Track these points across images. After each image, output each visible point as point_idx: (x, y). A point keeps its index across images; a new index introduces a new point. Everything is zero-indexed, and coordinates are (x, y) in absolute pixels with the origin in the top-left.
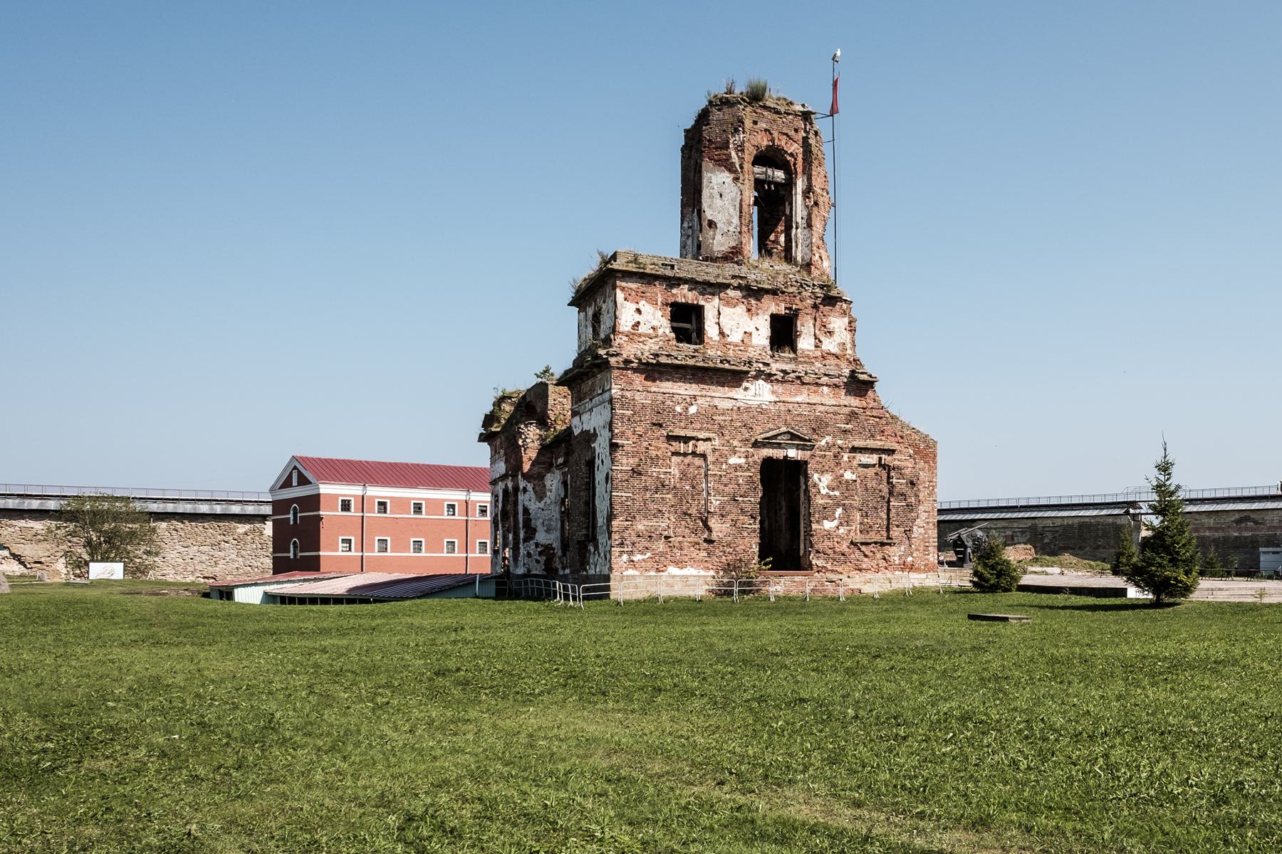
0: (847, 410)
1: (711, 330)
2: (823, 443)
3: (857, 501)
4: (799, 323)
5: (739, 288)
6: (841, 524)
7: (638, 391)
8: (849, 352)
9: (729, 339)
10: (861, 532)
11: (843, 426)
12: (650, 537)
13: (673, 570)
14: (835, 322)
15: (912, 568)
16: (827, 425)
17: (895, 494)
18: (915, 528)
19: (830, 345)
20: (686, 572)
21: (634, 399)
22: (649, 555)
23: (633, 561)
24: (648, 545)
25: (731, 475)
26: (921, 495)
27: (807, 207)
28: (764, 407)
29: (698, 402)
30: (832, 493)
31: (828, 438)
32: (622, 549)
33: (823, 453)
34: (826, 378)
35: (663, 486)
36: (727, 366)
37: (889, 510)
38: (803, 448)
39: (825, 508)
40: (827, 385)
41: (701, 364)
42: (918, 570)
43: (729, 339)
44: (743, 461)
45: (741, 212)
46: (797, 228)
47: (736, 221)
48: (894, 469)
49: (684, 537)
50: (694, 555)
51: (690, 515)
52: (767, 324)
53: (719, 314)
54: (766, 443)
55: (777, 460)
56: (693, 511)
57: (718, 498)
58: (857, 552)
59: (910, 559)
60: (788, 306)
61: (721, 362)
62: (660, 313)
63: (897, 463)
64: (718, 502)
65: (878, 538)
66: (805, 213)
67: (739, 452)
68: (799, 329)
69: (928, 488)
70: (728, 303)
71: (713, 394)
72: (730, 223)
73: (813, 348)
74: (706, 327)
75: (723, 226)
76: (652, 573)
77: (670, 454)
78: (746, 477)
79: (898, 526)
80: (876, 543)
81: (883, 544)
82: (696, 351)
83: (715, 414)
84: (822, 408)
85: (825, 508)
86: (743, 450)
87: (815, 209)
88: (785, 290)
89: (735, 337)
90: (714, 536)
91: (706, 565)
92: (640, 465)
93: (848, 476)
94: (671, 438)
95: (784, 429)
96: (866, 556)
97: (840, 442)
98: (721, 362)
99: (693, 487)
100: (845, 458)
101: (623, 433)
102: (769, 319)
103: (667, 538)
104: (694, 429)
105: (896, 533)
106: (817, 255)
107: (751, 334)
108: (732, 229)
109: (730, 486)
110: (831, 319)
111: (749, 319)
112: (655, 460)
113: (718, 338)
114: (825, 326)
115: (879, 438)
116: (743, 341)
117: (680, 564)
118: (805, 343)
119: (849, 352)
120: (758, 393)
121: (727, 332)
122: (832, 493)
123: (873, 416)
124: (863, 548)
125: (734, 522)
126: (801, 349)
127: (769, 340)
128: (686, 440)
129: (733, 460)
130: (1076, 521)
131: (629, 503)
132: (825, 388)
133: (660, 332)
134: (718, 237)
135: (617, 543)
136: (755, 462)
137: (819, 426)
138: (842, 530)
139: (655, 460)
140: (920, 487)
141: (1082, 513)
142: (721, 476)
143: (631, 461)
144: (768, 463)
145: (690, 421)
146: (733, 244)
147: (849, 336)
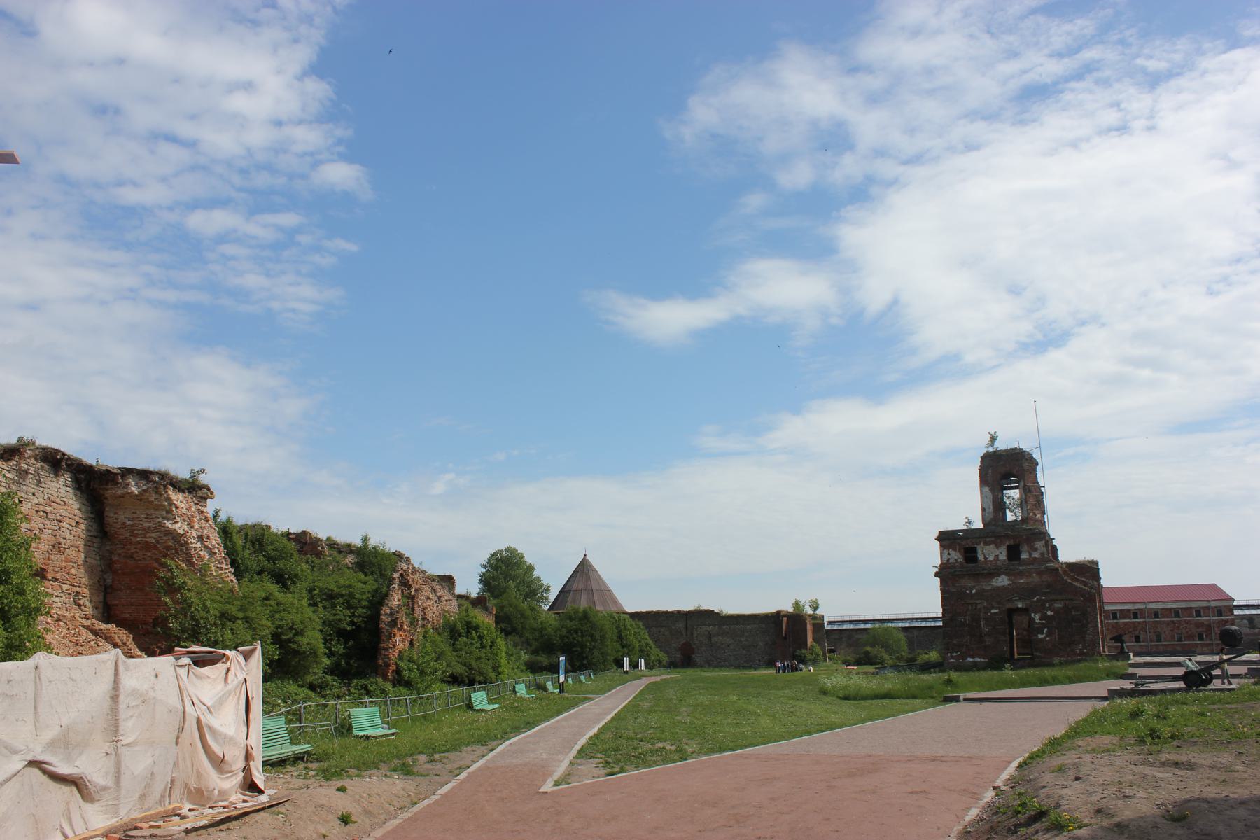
1: (981, 557)
4: (1020, 547)
6: (1047, 636)
13: (970, 659)
19: (1036, 555)
26: (1089, 620)
31: (1038, 597)
36: (985, 572)
44: (997, 611)
47: (991, 507)
52: (1006, 550)
59: (1085, 650)
70: (987, 544)
74: (978, 556)
93: (1049, 613)
95: (1015, 595)
100: (1047, 605)
106: (1031, 514)
107: (998, 556)
110: (1036, 543)
117: (973, 657)
118: (1024, 556)
119: (1046, 556)
120: (1003, 581)
128: (972, 604)
132: (1034, 575)
133: (959, 560)
137: (1031, 591)
147: (1045, 549)
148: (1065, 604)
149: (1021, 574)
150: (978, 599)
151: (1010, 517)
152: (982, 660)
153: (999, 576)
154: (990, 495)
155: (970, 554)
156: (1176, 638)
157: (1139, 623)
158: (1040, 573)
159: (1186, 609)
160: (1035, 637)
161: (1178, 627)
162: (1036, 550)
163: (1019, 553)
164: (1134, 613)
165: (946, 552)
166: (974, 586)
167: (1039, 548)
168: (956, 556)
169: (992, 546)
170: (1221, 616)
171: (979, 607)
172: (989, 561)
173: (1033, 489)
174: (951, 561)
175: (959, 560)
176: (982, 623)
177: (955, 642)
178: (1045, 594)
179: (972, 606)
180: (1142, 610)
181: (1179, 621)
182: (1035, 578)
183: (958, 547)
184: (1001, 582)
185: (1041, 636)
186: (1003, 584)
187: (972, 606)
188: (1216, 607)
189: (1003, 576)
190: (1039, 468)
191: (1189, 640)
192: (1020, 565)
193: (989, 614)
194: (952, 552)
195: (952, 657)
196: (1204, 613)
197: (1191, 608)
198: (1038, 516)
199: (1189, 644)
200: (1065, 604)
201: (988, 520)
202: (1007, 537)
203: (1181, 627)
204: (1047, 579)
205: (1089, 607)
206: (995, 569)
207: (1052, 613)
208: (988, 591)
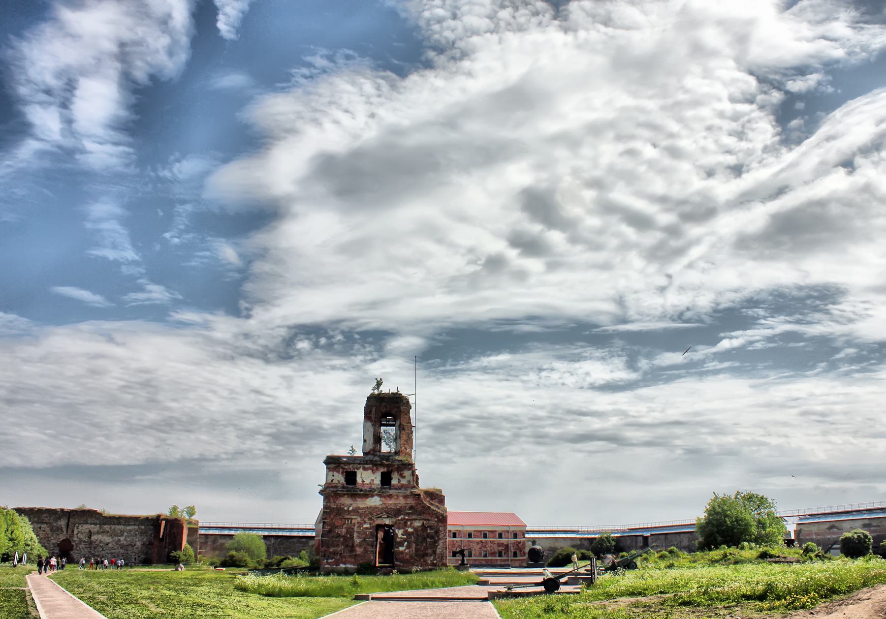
1: (359, 480)
4: (392, 474)
6: (406, 548)
8: (412, 483)
9: (365, 483)
13: (342, 566)
16: (402, 511)
18: (437, 550)
19: (404, 482)
22: (333, 560)
26: (440, 537)
30: (403, 537)
31: (402, 516)
34: (401, 494)
43: (365, 483)
44: (368, 526)
47: (372, 439)
59: (435, 562)
70: (365, 469)
73: (397, 483)
74: (357, 479)
76: (335, 566)
82: (352, 488)
84: (399, 505)
89: (367, 481)
93: (410, 530)
97: (406, 517)
104: (351, 515)
106: (403, 448)
107: (373, 480)
110: (404, 472)
112: (337, 527)
116: (370, 483)
117: (345, 563)
118: (394, 482)
120: (375, 501)
121: (364, 480)
122: (403, 537)
125: (365, 549)
128: (348, 519)
129: (365, 526)
133: (341, 482)
134: (367, 445)
136: (373, 526)
137: (398, 512)
143: (329, 527)
145: (349, 512)
148: (423, 523)
149: (390, 496)
150: (354, 515)
151: (385, 448)
152: (352, 566)
153: (372, 496)
154: (371, 429)
155: (351, 477)
156: (483, 554)
157: (457, 541)
158: (406, 497)
159: (492, 532)
160: (396, 549)
161: (485, 546)
163: (391, 479)
164: (453, 533)
165: (331, 473)
166: (351, 504)
167: (407, 476)
168: (339, 478)
170: (517, 538)
171: (353, 521)
172: (366, 484)
173: (406, 428)
174: (334, 482)
176: (355, 535)
177: (331, 550)
178: (409, 514)
179: (348, 521)
180: (460, 531)
181: (485, 541)
182: (402, 502)
183: (341, 470)
184: (374, 502)
185: (401, 549)
187: (348, 521)
188: (513, 531)
190: (412, 411)
191: (491, 556)
192: (390, 489)
193: (362, 528)
194: (335, 473)
195: (328, 563)
196: (505, 535)
197: (496, 531)
198: (408, 450)
199: (491, 560)
200: (423, 523)
201: (367, 450)
202: (382, 465)
203: (487, 546)
204: (411, 501)
205: (441, 526)
206: (370, 491)
208: (363, 509)
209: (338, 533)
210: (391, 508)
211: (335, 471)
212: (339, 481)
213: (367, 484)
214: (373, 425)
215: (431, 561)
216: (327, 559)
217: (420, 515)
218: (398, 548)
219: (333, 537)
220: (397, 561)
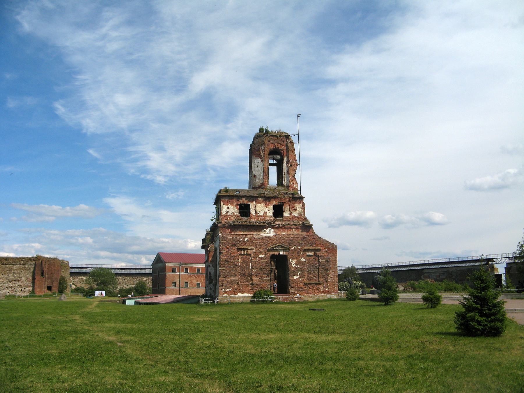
0: (301, 236)
1: (253, 212)
2: (293, 248)
3: (306, 268)
5: (261, 197)
6: (300, 277)
7: (228, 234)
10: (308, 279)
11: (300, 242)
12: (232, 283)
13: (240, 294)
14: (297, 206)
15: (328, 292)
17: (321, 266)
19: (295, 214)
20: (244, 295)
21: (226, 237)
22: (231, 289)
23: (226, 291)
24: (231, 286)
25: (260, 261)
26: (331, 266)
27: (288, 167)
28: (271, 237)
29: (248, 237)
30: (296, 266)
32: (222, 287)
33: (293, 252)
35: (236, 266)
37: (319, 271)
38: (286, 251)
39: (294, 272)
40: (294, 228)
41: (248, 224)
42: (330, 293)
43: (259, 215)
45: (264, 172)
46: (284, 174)
47: (262, 174)
48: (320, 256)
49: (243, 283)
50: (247, 289)
51: (246, 275)
52: (272, 208)
53: (255, 206)
54: (272, 249)
55: (276, 255)
56: (247, 274)
57: (255, 269)
58: (307, 287)
59: (327, 289)
60: (280, 201)
61: (255, 222)
62: (235, 208)
63: (321, 254)
64: (255, 271)
65: (314, 282)
66: (287, 169)
67: (263, 253)
68: (284, 209)
69: (334, 263)
70: (259, 203)
71: (253, 234)
72: (260, 175)
73: (289, 215)
74: (251, 211)
75: (258, 176)
76: (232, 295)
77: (238, 255)
78: (265, 261)
79: (322, 277)
80: (314, 284)
81: (316, 284)
82: (247, 219)
83: (254, 240)
84: (292, 236)
85: (294, 272)
86: (264, 252)
87: (291, 168)
88: (279, 196)
89: (261, 214)
90: (254, 282)
91: (251, 292)
92: (228, 259)
93: (303, 260)
94: (239, 250)
95: (278, 244)
96: (310, 288)
97: (299, 248)
98: (255, 222)
99: (247, 266)
100: (302, 254)
101: (223, 248)
102: (273, 207)
103: (238, 283)
105: (322, 279)
108: (261, 177)
109: (259, 265)
110: (296, 205)
111: (266, 208)
112: (233, 257)
113: (255, 215)
114: (293, 207)
115: (314, 246)
116: (264, 215)
118: (286, 214)
120: (270, 232)
121: (258, 212)
122: (296, 266)
123: (312, 238)
124: (309, 286)
125: (261, 277)
126: (285, 216)
127: (273, 214)
128: (244, 250)
130: (466, 268)
131: (224, 272)
132: (293, 229)
133: (235, 214)
134: (257, 180)
135: (221, 285)
136: (268, 256)
137: (292, 242)
138: (301, 279)
139: (233, 257)
140: (331, 262)
141: (468, 264)
142: (256, 261)
144: (273, 257)
145: (245, 243)
146: (261, 182)
147: (302, 210)
148: (315, 253)
149: (284, 227)
150: (249, 246)
155: (244, 210)
162: (296, 210)
169: (263, 204)
172: (259, 216)
175: (235, 214)
185: (295, 277)
186: (268, 235)
189: (270, 229)
195: (226, 292)
198: (295, 185)
200: (315, 253)
202: (274, 198)
207: (305, 260)
208: (257, 239)
209: (234, 263)
210: (284, 239)
211: (229, 203)
212: (233, 213)
213: (261, 216)
214: (262, 161)
215: (323, 288)
216: (225, 289)
217: (312, 245)
218: (292, 277)
219: (230, 267)
220: (292, 289)
